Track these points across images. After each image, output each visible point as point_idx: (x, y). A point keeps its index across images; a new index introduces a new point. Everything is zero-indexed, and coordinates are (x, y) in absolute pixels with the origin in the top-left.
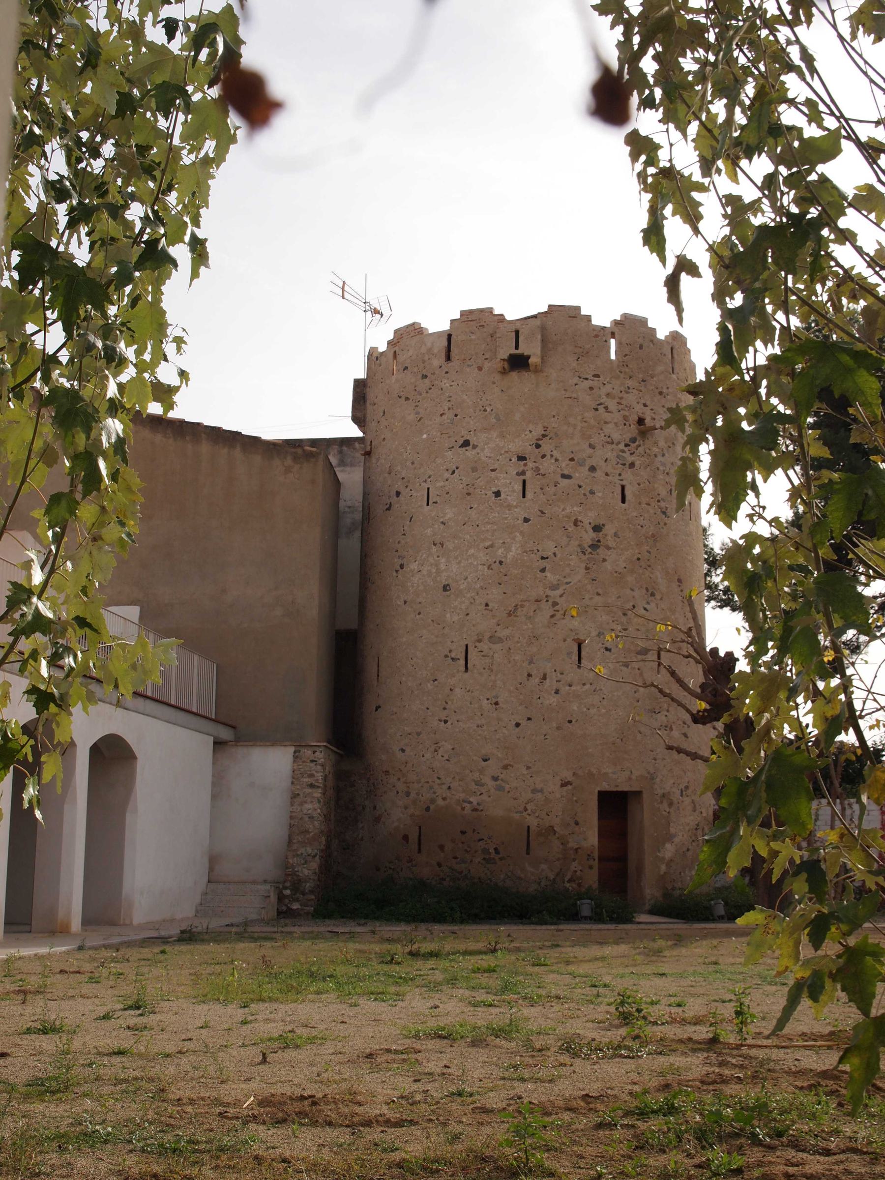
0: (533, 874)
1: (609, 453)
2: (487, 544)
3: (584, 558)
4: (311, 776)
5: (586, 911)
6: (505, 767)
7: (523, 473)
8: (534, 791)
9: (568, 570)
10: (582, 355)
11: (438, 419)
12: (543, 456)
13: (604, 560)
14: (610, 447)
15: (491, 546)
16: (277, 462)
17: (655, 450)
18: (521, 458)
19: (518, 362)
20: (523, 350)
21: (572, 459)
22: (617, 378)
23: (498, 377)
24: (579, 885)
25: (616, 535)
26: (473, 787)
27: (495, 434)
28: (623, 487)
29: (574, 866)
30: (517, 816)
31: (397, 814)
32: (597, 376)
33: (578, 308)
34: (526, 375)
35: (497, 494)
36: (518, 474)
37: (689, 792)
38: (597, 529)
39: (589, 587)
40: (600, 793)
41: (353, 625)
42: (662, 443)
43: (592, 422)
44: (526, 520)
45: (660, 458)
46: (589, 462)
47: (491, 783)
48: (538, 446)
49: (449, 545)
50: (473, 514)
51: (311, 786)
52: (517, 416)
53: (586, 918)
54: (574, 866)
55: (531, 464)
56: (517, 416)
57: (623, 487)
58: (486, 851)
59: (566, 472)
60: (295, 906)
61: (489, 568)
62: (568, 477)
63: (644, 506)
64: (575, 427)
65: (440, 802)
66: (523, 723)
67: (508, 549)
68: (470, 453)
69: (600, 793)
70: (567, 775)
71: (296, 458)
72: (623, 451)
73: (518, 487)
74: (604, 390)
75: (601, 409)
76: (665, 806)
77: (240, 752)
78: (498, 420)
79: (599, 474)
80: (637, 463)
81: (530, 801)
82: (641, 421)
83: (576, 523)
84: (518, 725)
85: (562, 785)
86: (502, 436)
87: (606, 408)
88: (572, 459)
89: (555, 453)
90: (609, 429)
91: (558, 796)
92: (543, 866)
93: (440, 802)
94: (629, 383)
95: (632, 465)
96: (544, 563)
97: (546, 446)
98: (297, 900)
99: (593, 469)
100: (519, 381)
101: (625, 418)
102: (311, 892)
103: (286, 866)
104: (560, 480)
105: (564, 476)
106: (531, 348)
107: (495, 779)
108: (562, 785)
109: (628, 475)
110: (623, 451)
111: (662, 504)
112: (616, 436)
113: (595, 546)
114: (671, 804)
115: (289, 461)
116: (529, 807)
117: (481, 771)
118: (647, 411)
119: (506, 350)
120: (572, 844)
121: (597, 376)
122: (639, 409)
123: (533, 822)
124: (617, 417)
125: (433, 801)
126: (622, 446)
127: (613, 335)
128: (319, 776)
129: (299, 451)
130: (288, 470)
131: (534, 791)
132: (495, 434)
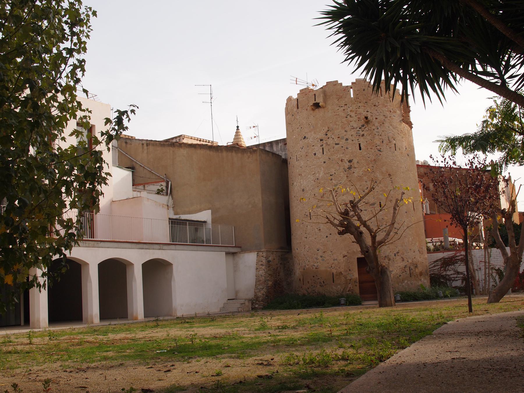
0: (335, 289)
1: (353, 132)
2: (313, 173)
3: (346, 173)
4: (262, 261)
5: (343, 302)
6: (324, 252)
7: (322, 145)
8: (334, 260)
9: (340, 178)
10: (339, 98)
11: (297, 130)
12: (328, 138)
13: (354, 173)
14: (353, 130)
15: (315, 173)
16: (245, 155)
17: (374, 127)
18: (321, 140)
19: (317, 106)
20: (317, 101)
21: (339, 137)
22: (354, 104)
23: (312, 112)
24: (352, 292)
25: (358, 162)
26: (315, 260)
27: (313, 133)
28: (360, 144)
29: (350, 286)
30: (329, 269)
31: (298, 272)
32: (346, 105)
33: (337, 81)
34: (320, 109)
35: (315, 154)
36: (321, 146)
37: (399, 254)
38: (350, 161)
39: (348, 183)
40: (358, 258)
41: (99, 235)
42: (377, 124)
43: (345, 122)
44: (324, 162)
45: (376, 130)
46: (345, 137)
47: (320, 258)
48: (326, 135)
49: (303, 175)
50: (308, 162)
51: (262, 265)
52: (319, 125)
53: (343, 304)
54: (350, 286)
55: (325, 142)
56: (319, 125)
57: (360, 144)
58: (320, 283)
59: (337, 143)
60: (257, 306)
61: (315, 181)
62: (338, 144)
63: (369, 149)
64: (339, 125)
65: (307, 267)
66: (329, 236)
67: (319, 174)
68: (306, 141)
69: (358, 258)
70: (345, 253)
71: (251, 153)
72: (359, 131)
73: (321, 151)
74: (349, 110)
75: (349, 117)
76: (387, 260)
77: (242, 255)
78: (313, 127)
79: (349, 141)
80: (365, 134)
81: (333, 263)
82: (366, 118)
83: (342, 161)
84: (327, 237)
85: (344, 257)
86: (315, 133)
87: (350, 116)
88: (339, 137)
89: (332, 136)
90: (351, 124)
91: (342, 261)
92: (339, 286)
93: (307, 267)
94: (360, 104)
95: (363, 135)
96: (331, 177)
97: (329, 134)
98: (257, 304)
99: (347, 139)
100: (319, 112)
101: (359, 118)
102: (262, 301)
103: (255, 293)
104: (335, 146)
105: (336, 144)
106: (320, 100)
107: (321, 257)
108: (344, 257)
109: (362, 140)
110: (359, 131)
111: (378, 147)
112: (355, 126)
113: (350, 168)
114: (389, 260)
115: (249, 154)
116: (333, 266)
117: (317, 255)
118: (369, 113)
119: (312, 102)
120: (349, 278)
121: (346, 105)
122: (365, 114)
123: (334, 271)
124: (356, 118)
125: (305, 266)
126: (358, 129)
127: (351, 88)
128: (264, 261)
129: (251, 150)
130: (249, 157)
131: (334, 260)
132: (313, 133)
